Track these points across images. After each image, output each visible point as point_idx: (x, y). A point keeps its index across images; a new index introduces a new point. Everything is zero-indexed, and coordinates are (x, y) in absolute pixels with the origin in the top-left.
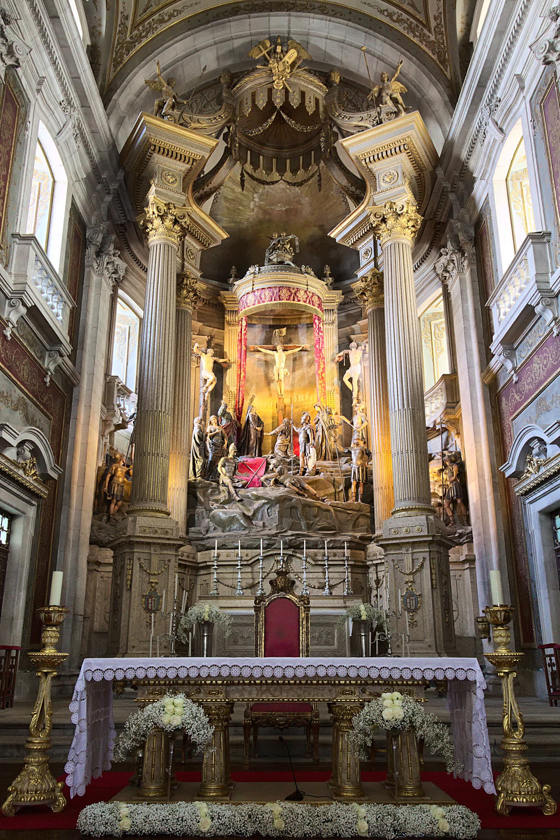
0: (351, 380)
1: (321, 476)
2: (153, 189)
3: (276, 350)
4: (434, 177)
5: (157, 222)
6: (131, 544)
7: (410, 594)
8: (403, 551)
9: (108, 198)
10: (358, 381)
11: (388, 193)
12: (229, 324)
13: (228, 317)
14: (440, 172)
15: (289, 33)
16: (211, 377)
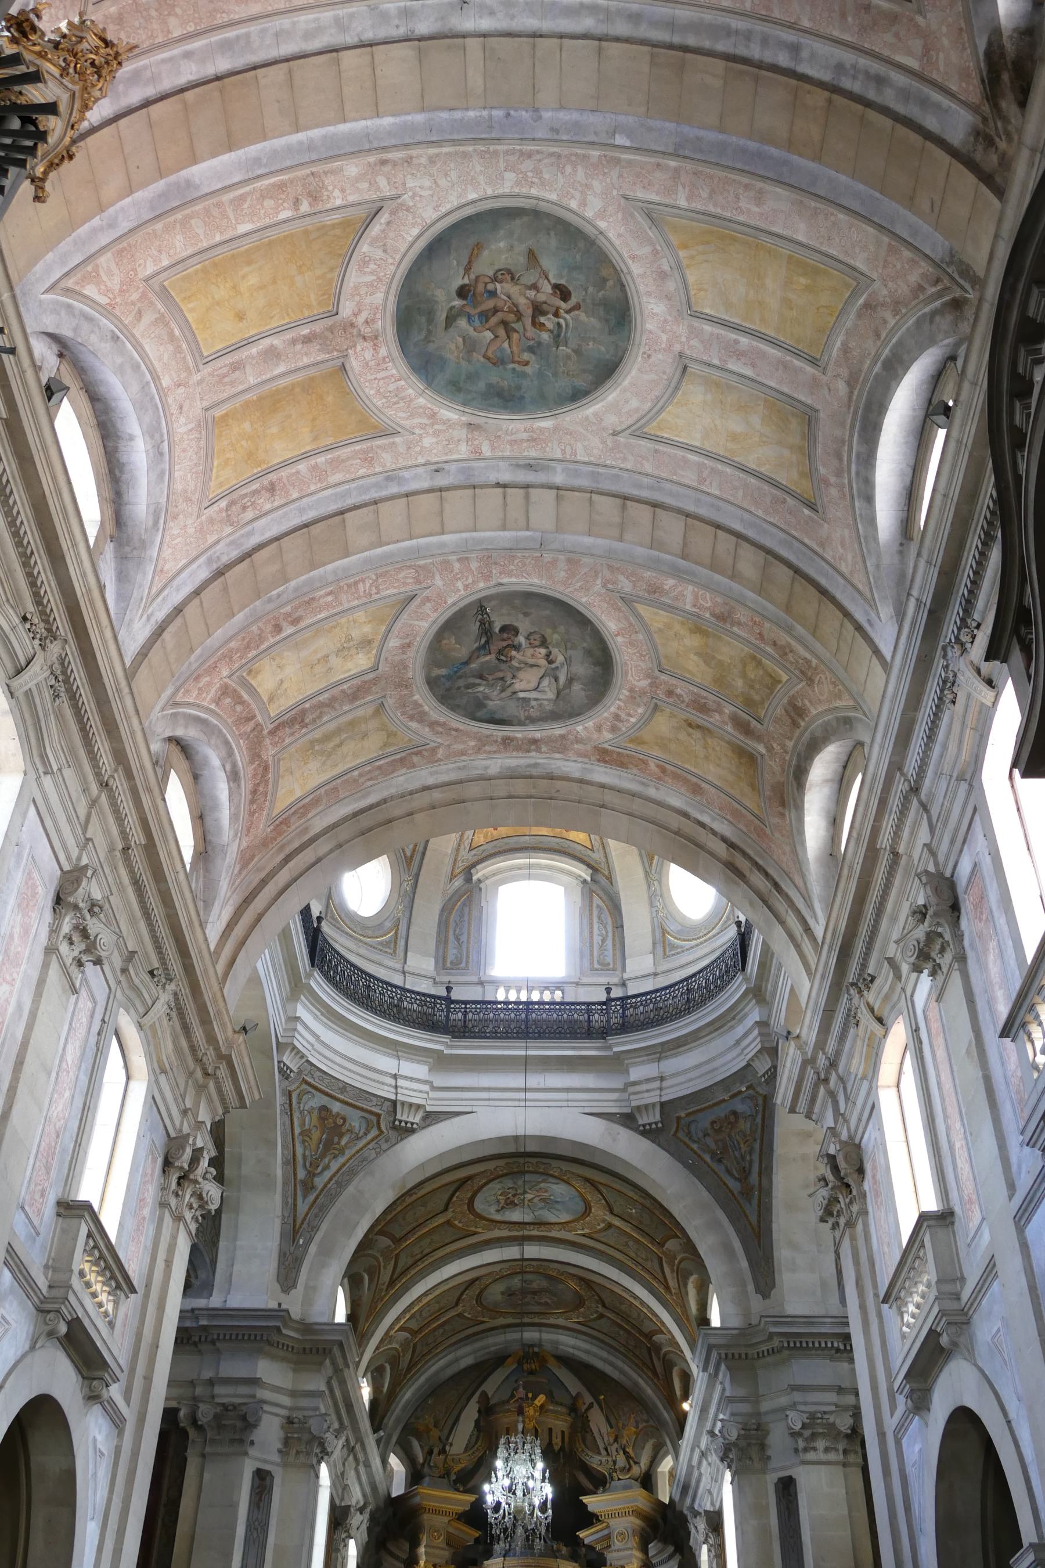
2: (422, 1550)
15: (540, 1339)
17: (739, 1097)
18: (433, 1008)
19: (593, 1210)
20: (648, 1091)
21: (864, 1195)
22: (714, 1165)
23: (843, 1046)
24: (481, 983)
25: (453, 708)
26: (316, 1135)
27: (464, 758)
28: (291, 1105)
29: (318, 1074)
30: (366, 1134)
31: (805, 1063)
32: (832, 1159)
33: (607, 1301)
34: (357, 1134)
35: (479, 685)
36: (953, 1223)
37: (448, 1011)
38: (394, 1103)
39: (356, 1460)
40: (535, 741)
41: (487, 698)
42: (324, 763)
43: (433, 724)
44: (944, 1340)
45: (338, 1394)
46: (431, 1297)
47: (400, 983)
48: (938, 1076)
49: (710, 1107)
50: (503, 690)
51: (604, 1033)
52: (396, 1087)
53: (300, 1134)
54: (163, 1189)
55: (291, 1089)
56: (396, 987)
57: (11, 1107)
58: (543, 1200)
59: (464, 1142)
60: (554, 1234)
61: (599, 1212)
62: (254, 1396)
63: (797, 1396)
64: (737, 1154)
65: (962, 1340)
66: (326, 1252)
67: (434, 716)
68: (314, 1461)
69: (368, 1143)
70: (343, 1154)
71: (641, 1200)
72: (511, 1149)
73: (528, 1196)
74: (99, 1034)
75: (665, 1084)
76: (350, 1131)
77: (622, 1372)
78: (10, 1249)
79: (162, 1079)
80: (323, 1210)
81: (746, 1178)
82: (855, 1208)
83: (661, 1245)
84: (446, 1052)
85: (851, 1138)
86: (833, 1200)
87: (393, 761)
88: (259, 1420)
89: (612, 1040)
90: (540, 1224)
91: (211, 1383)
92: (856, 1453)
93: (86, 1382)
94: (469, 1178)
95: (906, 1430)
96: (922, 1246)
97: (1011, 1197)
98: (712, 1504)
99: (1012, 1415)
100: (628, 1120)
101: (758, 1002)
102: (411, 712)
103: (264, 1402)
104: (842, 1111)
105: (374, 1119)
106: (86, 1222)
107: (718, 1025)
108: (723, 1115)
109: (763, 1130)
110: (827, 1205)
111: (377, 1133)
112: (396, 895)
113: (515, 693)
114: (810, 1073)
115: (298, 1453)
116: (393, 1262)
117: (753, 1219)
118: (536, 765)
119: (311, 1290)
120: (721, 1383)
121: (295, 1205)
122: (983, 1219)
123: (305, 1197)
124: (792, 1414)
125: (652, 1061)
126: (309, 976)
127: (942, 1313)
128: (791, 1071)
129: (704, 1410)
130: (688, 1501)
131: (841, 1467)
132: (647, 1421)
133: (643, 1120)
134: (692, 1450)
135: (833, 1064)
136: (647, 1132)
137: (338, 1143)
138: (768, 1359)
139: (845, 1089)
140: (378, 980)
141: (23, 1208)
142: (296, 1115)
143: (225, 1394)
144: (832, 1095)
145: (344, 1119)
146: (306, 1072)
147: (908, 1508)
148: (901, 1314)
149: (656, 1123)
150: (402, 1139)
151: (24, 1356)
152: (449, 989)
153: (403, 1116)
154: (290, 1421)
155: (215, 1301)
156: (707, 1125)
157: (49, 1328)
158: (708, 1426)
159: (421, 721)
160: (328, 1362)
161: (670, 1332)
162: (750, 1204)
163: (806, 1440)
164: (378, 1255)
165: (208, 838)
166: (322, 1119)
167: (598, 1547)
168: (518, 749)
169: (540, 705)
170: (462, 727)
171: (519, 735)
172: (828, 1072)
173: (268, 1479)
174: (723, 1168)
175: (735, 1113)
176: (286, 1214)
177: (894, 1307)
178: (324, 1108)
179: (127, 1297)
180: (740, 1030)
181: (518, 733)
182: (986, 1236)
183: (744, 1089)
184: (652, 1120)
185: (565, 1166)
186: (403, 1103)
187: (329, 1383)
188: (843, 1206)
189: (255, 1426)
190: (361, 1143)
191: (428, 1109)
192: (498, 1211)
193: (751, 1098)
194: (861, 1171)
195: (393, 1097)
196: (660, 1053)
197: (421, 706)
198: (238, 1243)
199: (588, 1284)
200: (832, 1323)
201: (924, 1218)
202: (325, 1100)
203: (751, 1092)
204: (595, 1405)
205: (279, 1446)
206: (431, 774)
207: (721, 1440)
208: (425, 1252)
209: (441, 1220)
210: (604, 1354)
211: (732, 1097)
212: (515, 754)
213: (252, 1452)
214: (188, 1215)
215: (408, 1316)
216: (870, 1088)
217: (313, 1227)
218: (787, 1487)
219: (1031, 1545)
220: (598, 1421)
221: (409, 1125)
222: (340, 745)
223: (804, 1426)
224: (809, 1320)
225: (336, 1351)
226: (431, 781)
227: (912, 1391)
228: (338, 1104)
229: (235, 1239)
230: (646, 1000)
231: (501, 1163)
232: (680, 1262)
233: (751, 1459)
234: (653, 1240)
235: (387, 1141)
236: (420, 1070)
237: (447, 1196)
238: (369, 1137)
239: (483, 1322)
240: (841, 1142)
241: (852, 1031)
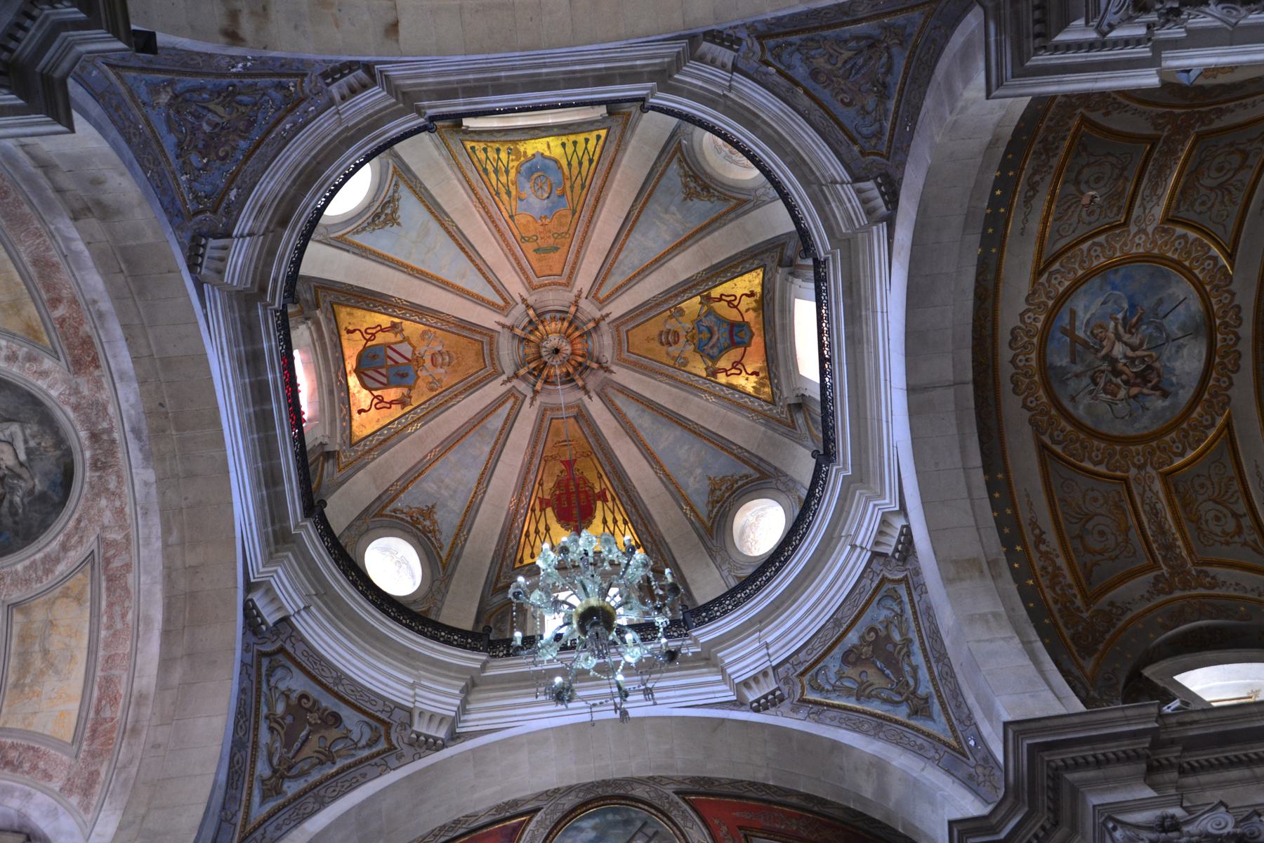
17: (790, 73)
20: (850, 201)
25: (45, 526)
26: (872, 676)
27: (127, 510)
28: (816, 703)
35: (11, 502)
38: (875, 555)
40: (95, 437)
41: (31, 492)
42: (57, 672)
43: (65, 548)
50: (19, 477)
53: (858, 699)
64: (861, 61)
67: (55, 545)
69: (911, 600)
73: (1119, 350)
76: (888, 624)
80: (957, 693)
87: (108, 589)
102: (40, 573)
109: (803, 31)
111: (904, 585)
112: (783, 497)
113: (21, 464)
116: (1212, 570)
118: (136, 432)
121: (929, 735)
123: (930, 717)
126: (696, 642)
136: (892, 199)
137: (895, 645)
145: (872, 629)
146: (792, 670)
149: (879, 186)
153: (890, 545)
156: (851, 111)
159: (57, 561)
164: (1162, 598)
165: (16, 827)
168: (111, 452)
169: (34, 437)
170: (76, 516)
171: (88, 454)
174: (889, 79)
175: (814, 74)
176: (932, 753)
178: (845, 659)
181: (84, 455)
184: (876, 193)
186: (876, 543)
193: (778, 57)
195: (869, 554)
197: (34, 562)
202: (838, 652)
206: (148, 543)
208: (1242, 508)
211: (797, 84)
212: (120, 455)
222: (45, 652)
225: (1057, 758)
226: (159, 544)
228: (850, 635)
238: (906, 599)
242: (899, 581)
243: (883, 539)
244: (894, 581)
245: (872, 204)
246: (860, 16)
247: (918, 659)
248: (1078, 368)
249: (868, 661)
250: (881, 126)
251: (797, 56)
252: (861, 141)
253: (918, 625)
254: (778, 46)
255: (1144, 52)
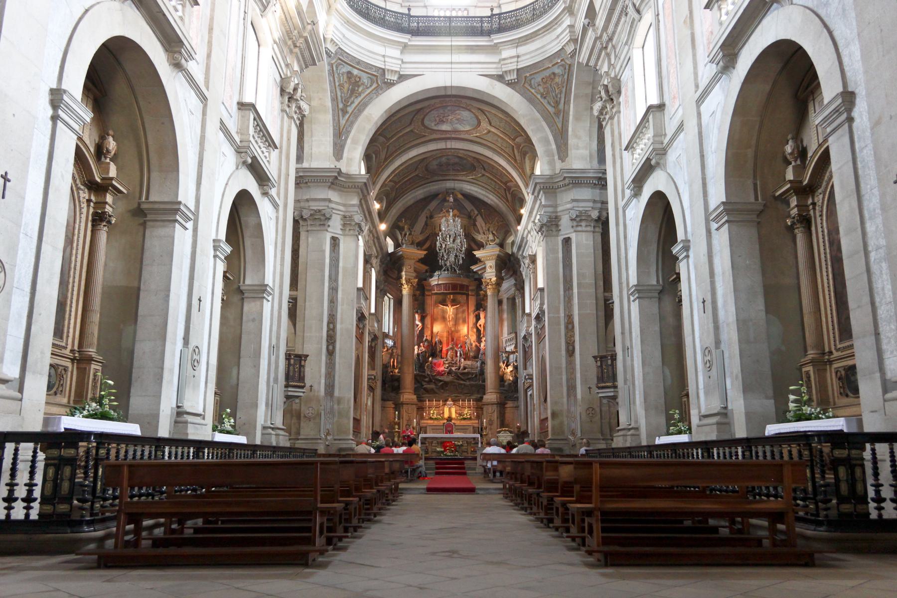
0: (480, 325)
1: (466, 371)
2: (403, 273)
3: (447, 305)
4: (510, 260)
5: (405, 286)
6: (402, 404)
7: (490, 420)
8: (489, 406)
9: (383, 266)
10: (484, 326)
11: (489, 274)
12: (427, 295)
13: (427, 293)
14: (512, 259)
16: (420, 324)
17: (557, 66)
18: (401, 20)
19: (482, 124)
20: (511, 63)
21: (619, 104)
22: (542, 100)
23: (617, 29)
24: (426, 7)
26: (346, 86)
29: (345, 54)
30: (371, 86)
31: (596, 39)
32: (606, 87)
33: (486, 168)
34: (366, 86)
36: (664, 110)
37: (409, 22)
38: (384, 70)
39: (373, 236)
44: (653, 162)
45: (364, 206)
46: (404, 166)
47: (384, 7)
48: (666, 37)
49: (541, 71)
51: (489, 33)
52: (385, 62)
54: (282, 103)
55: (333, 62)
56: (382, 8)
57: (211, 52)
58: (457, 119)
59: (418, 90)
60: (462, 136)
61: (485, 125)
62: (328, 207)
63: (575, 204)
65: (662, 162)
66: (355, 142)
68: (357, 233)
70: (360, 96)
71: (505, 118)
72: (442, 93)
73: (450, 117)
74: (244, 19)
75: (519, 59)
77: (492, 200)
78: (222, 122)
79: (275, 45)
80: (352, 123)
81: (558, 106)
82: (614, 110)
83: (514, 140)
84: (409, 43)
85: (616, 76)
86: (604, 108)
88: (331, 216)
89: (493, 37)
90: (456, 131)
91: (307, 200)
92: (599, 227)
93: (261, 187)
94: (421, 109)
95: (629, 206)
96: (648, 121)
97: (696, 92)
98: (532, 252)
99: (681, 191)
100: (500, 78)
101: (570, 15)
103: (333, 209)
104: (612, 63)
105: (375, 78)
106: (252, 112)
107: (548, 28)
108: (548, 75)
110: (601, 110)
111: (377, 85)
114: (598, 43)
115: (350, 230)
116: (386, 150)
117: (560, 125)
119: (350, 160)
120: (540, 200)
121: (339, 121)
122: (680, 105)
124: (571, 211)
125: (513, 48)
127: (654, 150)
128: (588, 44)
129: (531, 212)
130: (520, 253)
131: (592, 233)
132: (502, 221)
133: (508, 78)
134: (524, 230)
135: (610, 39)
136: (510, 84)
137: (358, 90)
138: (562, 189)
139: (615, 52)
140: (373, 4)
141: (223, 103)
142: (336, 75)
143: (315, 206)
144: (608, 55)
145: (360, 78)
147: (625, 237)
148: (633, 154)
149: (514, 79)
150: (389, 89)
151: (234, 172)
152: (409, 9)
153: (390, 77)
154: (345, 217)
155: (305, 165)
156: (539, 79)
157: (244, 160)
158: (532, 219)
160: (360, 192)
161: (516, 181)
162: (559, 118)
163: (577, 222)
166: (349, 78)
167: (480, 272)
172: (607, 43)
173: (337, 240)
174: (546, 101)
175: (554, 74)
177: (630, 151)
178: (349, 73)
179: (274, 151)
180: (559, 30)
182: (680, 112)
183: (559, 61)
184: (512, 78)
185: (468, 102)
186: (388, 70)
187: (360, 201)
188: (608, 109)
189: (329, 219)
190: (368, 91)
191: (401, 73)
192: (435, 125)
194: (619, 92)
195: (383, 67)
196: (518, 43)
198: (314, 139)
199: (478, 160)
200: (593, 172)
201: (650, 108)
202: (350, 68)
203: (563, 62)
204: (479, 215)
205: (341, 227)
207: (540, 223)
209: (408, 130)
210: (484, 193)
211: (553, 65)
213: (329, 229)
214: (295, 117)
215: (393, 175)
216: (629, 49)
217: (348, 131)
218: (567, 241)
219: (682, 241)
220: (480, 222)
221: (392, 81)
223: (577, 216)
224: (583, 171)
227: (634, 187)
228: (356, 70)
229: (312, 136)
230: (511, 15)
231: (438, 101)
232: (524, 146)
233: (552, 230)
234: (510, 138)
235: (381, 90)
236: (395, 52)
237: (412, 117)
239: (427, 179)
240: (610, 77)
241: (623, 19)
242: (377, 83)
243: (390, 72)
244: (377, 80)
245: (508, 74)
246: (566, 105)
247: (357, 102)
248: (446, 111)
249: (350, 83)
250: (533, 89)
251: (561, 73)
252: (530, 78)
253: (366, 96)
254: (565, 69)
255: (536, 194)
